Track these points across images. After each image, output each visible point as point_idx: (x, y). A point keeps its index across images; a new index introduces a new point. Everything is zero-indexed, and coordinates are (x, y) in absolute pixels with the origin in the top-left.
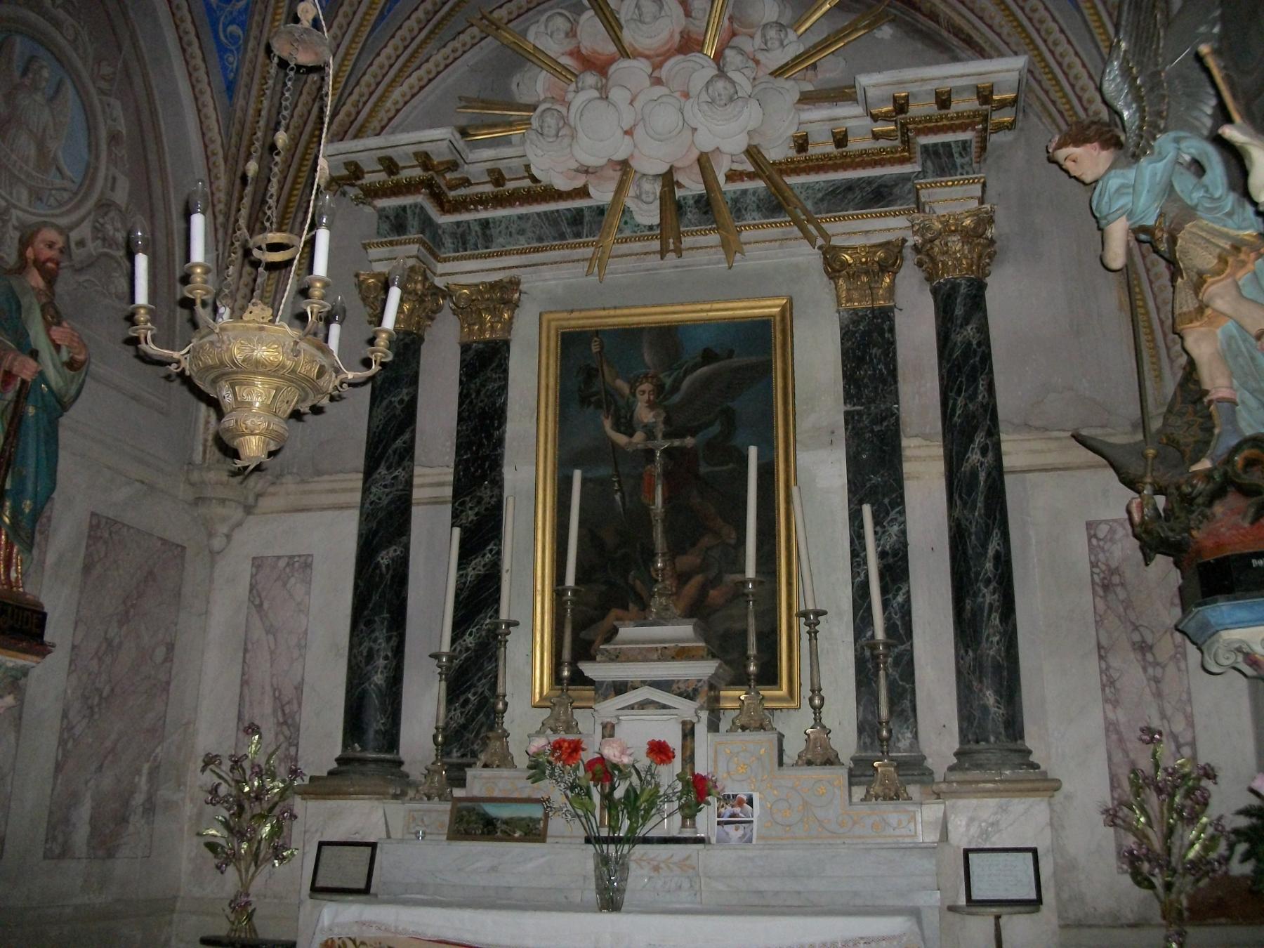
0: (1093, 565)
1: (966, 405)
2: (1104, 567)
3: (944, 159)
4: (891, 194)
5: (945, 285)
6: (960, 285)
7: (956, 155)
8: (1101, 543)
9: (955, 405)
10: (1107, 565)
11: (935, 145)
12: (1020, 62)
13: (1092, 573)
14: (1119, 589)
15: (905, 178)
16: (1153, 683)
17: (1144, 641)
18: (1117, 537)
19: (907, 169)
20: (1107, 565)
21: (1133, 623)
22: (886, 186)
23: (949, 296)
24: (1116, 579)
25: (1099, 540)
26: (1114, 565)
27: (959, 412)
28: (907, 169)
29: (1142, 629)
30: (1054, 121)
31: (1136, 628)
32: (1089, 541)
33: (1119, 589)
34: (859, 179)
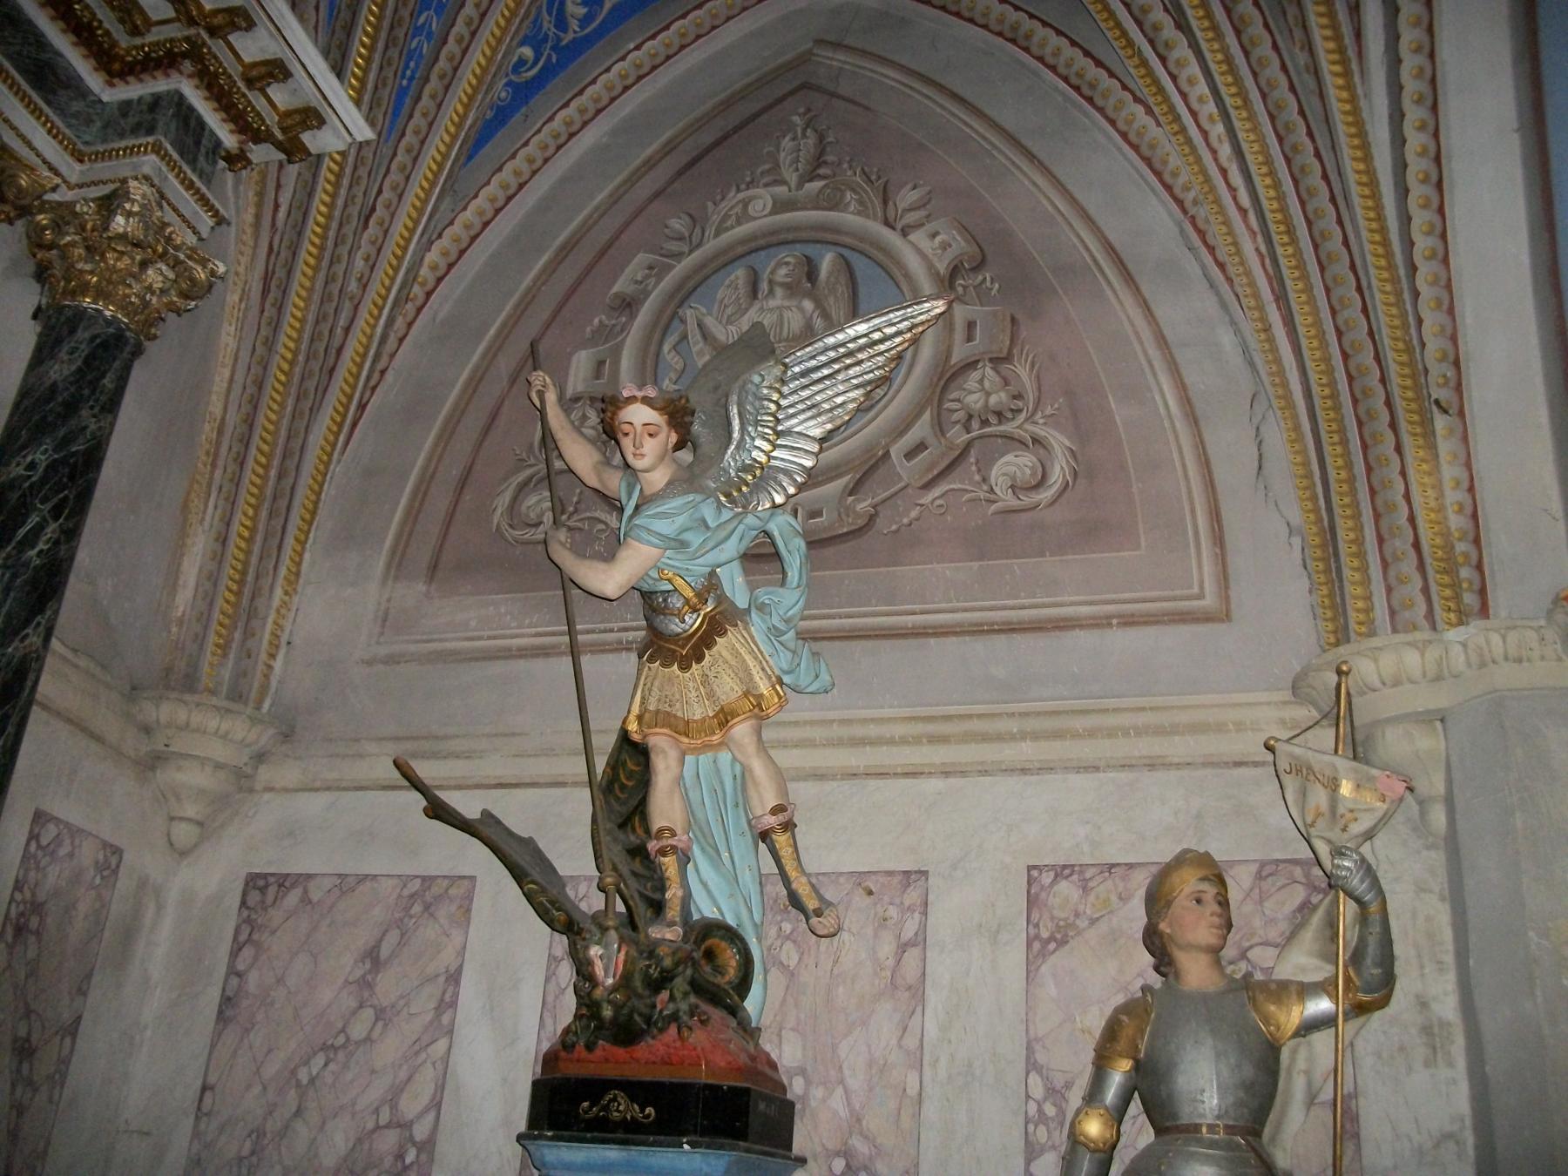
0: (18, 886)
1: (57, 543)
2: (28, 895)
3: (190, 141)
4: (54, 92)
5: (108, 323)
6: (127, 342)
7: (203, 150)
8: (40, 853)
9: (38, 530)
10: (33, 895)
11: (191, 109)
12: (364, 132)
13: (12, 900)
14: (32, 939)
15: (83, 92)
16: (14, 1113)
17: (28, 1040)
18: (62, 852)
19: (93, 80)
20: (33, 895)
21: (27, 1005)
22: (55, 74)
23: (105, 345)
24: (34, 922)
25: (39, 847)
26: (41, 897)
27: (41, 546)
28: (93, 80)
29: (33, 1017)
30: (259, 205)
31: (28, 1013)
32: (28, 844)
33: (32, 939)
34: (30, 22)
